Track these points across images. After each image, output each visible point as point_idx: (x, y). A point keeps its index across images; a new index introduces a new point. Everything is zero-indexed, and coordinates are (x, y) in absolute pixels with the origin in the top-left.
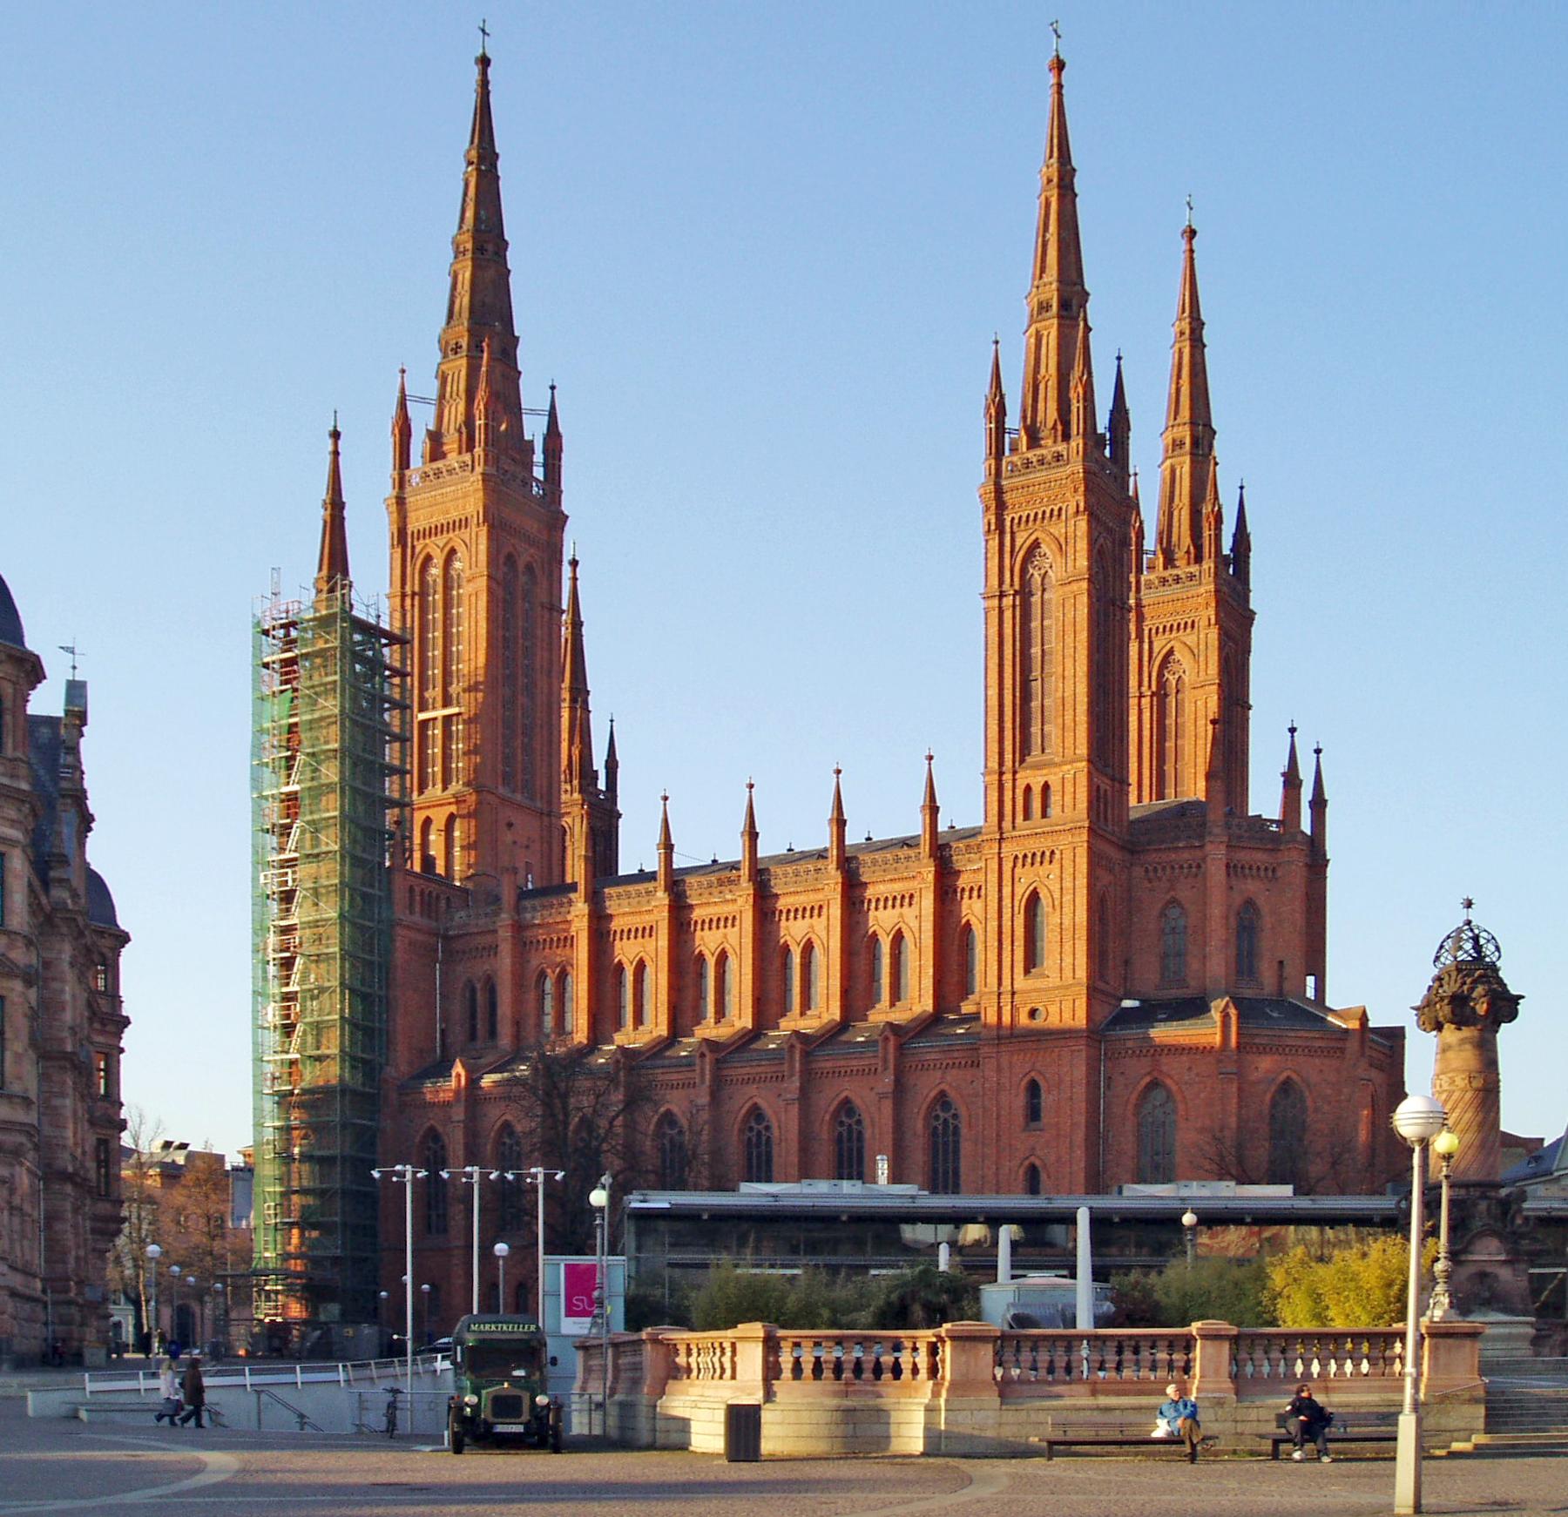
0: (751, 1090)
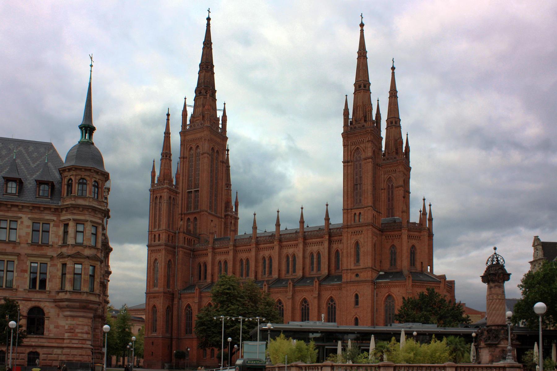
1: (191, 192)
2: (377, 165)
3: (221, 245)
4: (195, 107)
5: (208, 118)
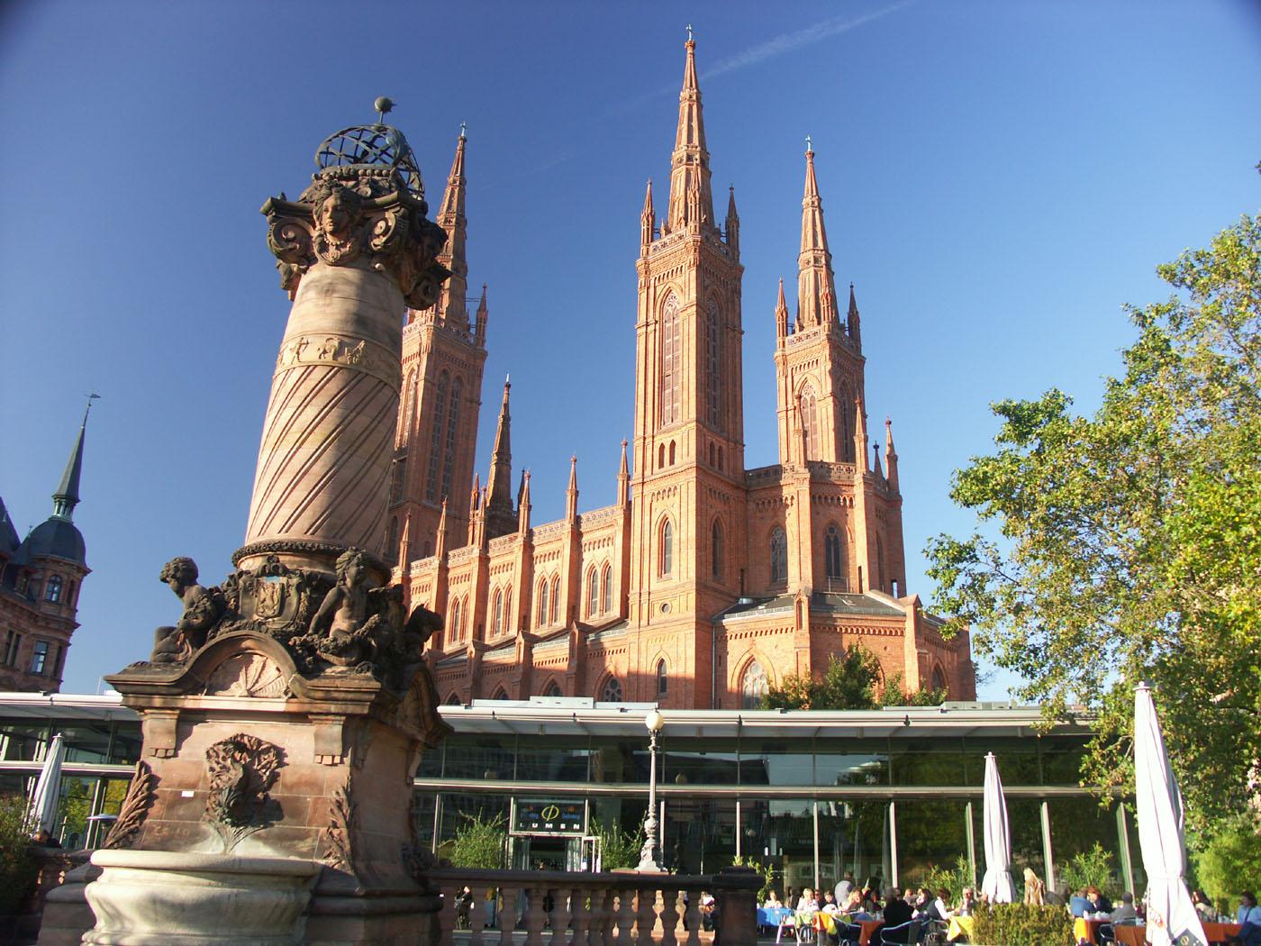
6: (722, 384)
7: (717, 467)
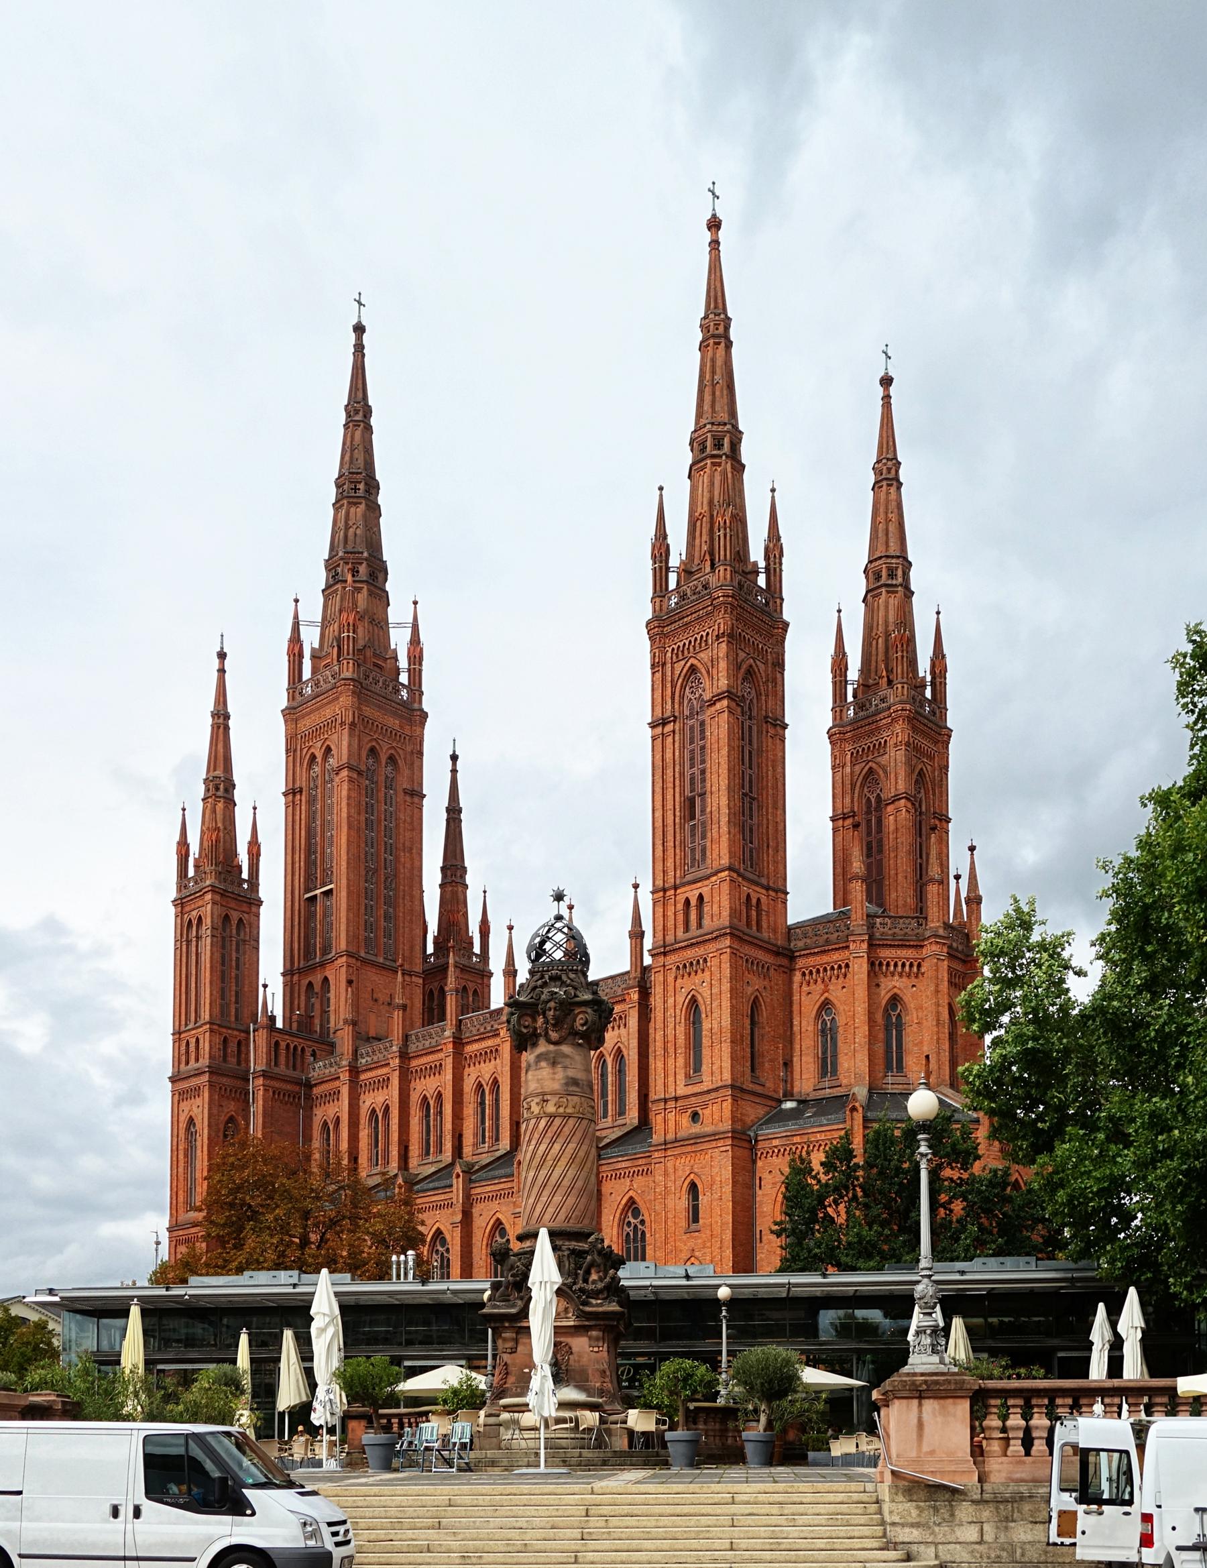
0: (494, 1205)
1: (316, 896)
2: (767, 722)
3: (375, 1058)
4: (325, 624)
5: (348, 654)
6: (760, 808)
7: (755, 928)
